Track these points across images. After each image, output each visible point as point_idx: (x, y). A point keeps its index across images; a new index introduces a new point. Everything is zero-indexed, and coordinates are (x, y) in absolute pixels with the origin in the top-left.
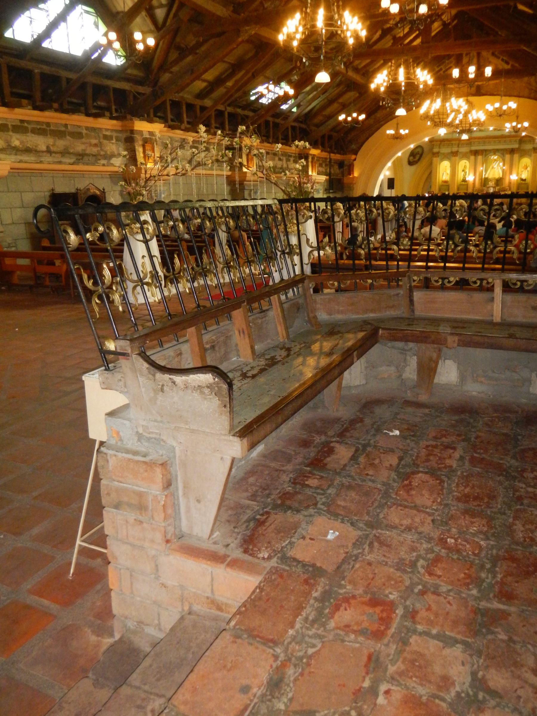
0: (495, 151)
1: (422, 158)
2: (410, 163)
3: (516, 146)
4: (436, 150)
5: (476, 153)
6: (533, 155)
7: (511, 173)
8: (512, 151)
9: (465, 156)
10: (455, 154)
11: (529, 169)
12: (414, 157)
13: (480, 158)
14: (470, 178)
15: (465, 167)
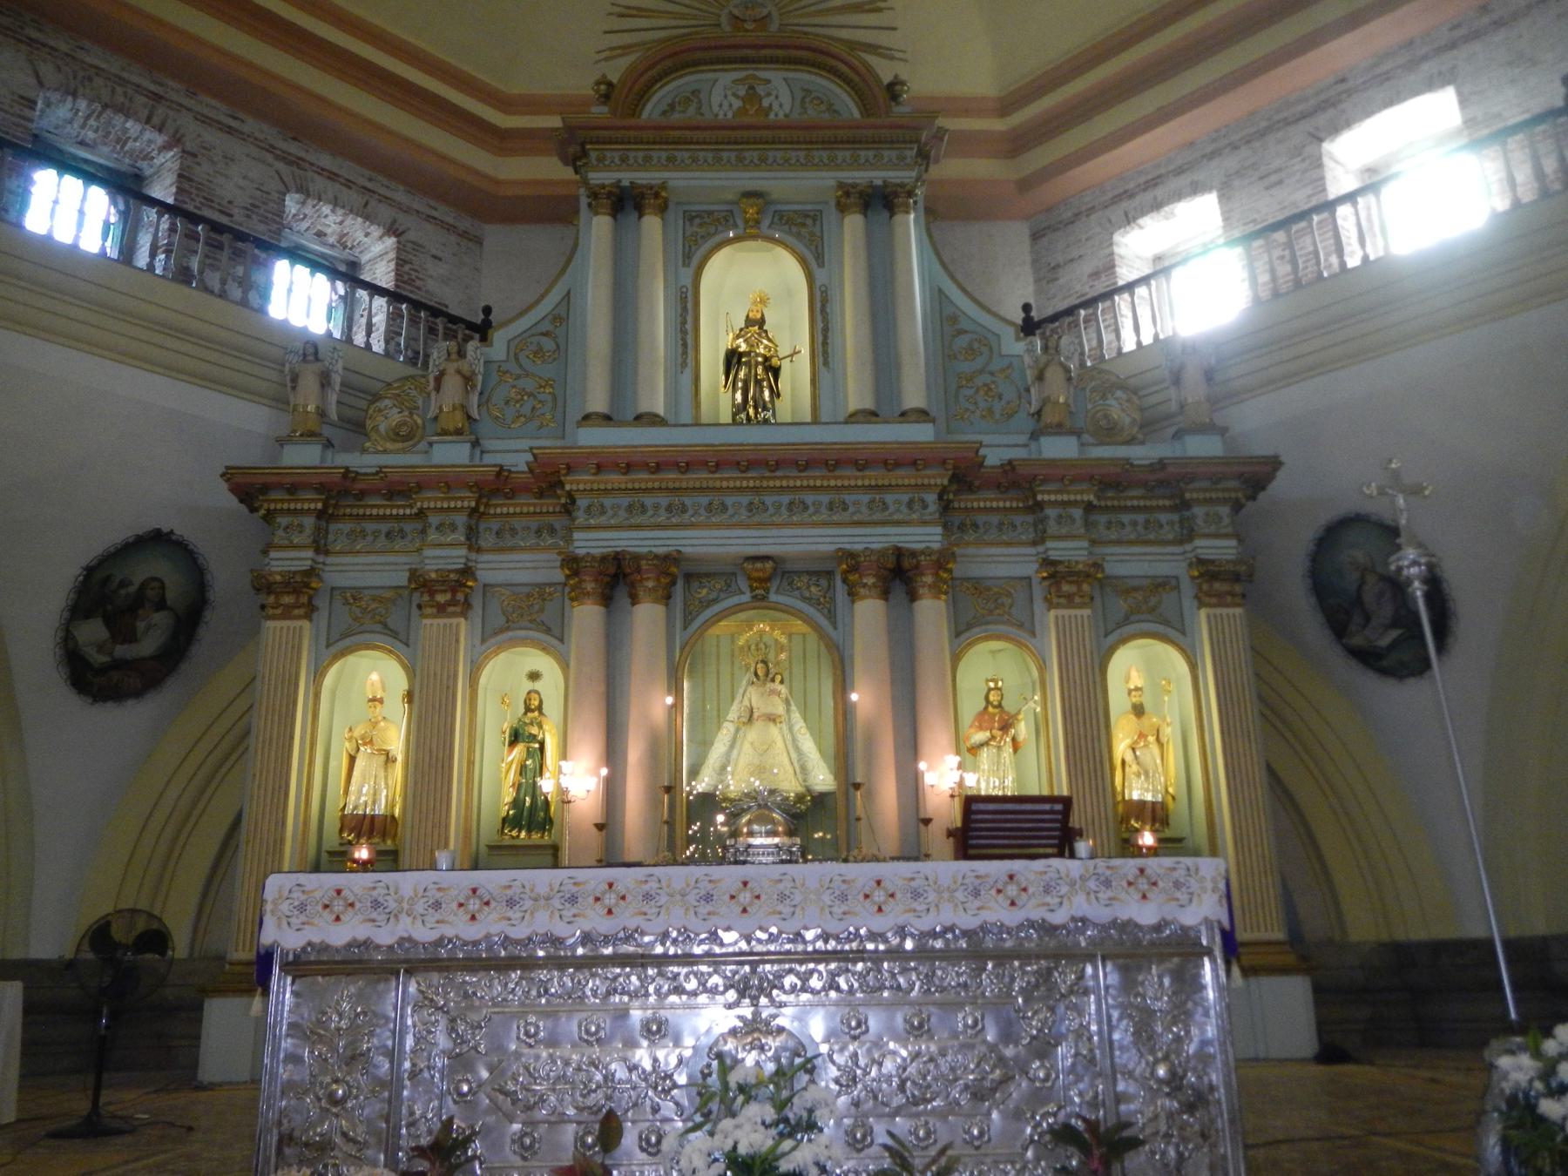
0: (765, 579)
1: (200, 650)
2: (94, 679)
3: (924, 537)
4: (287, 561)
5: (616, 580)
6: (1050, 620)
7: (910, 748)
8: (898, 576)
9: (532, 616)
10: (449, 593)
11: (1023, 729)
12: (121, 629)
13: (647, 618)
14: (576, 779)
15: (533, 707)
